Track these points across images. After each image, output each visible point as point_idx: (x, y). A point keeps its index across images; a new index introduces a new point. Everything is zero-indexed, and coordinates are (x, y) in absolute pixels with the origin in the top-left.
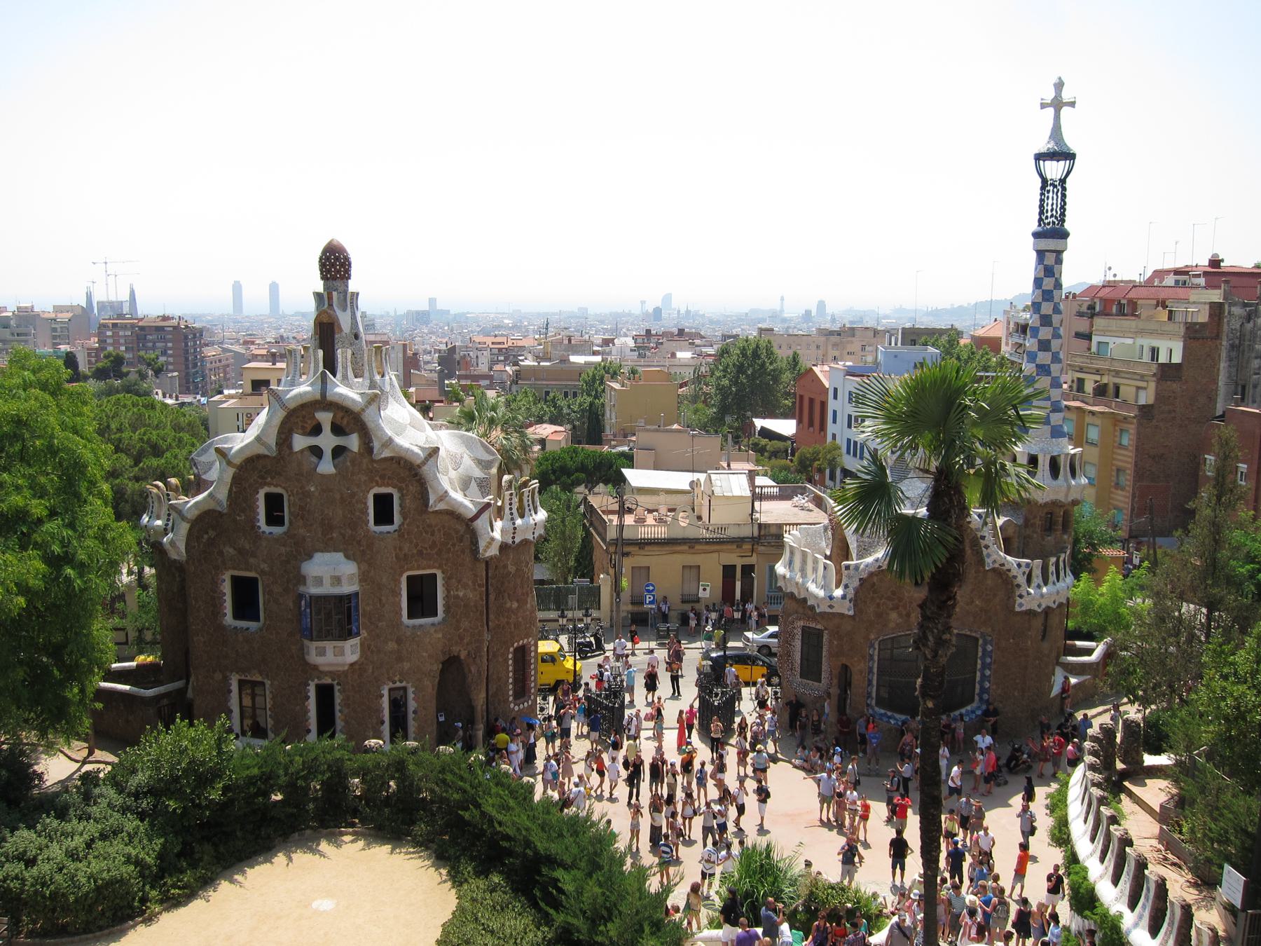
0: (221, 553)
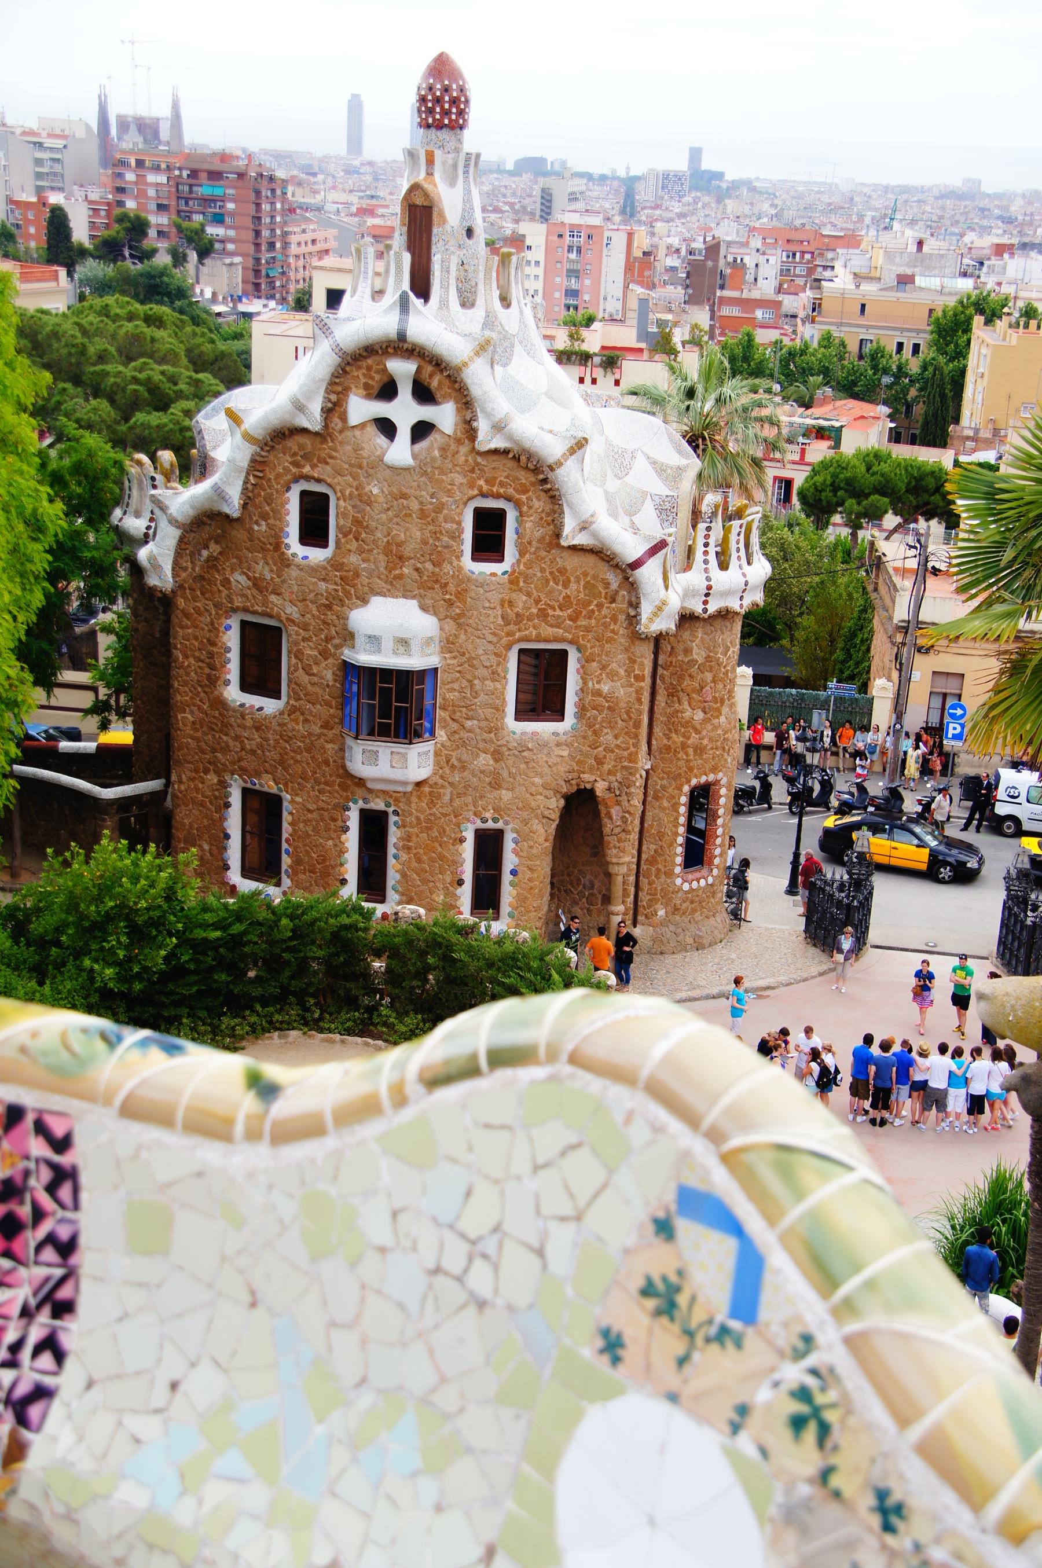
0: (229, 582)
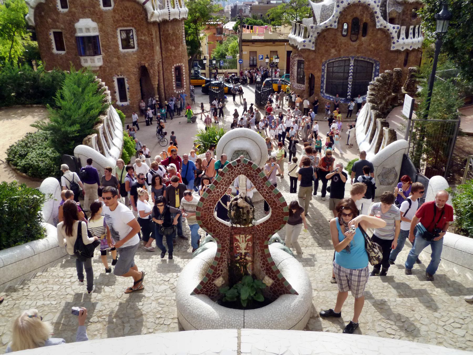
0: (47, 22)
